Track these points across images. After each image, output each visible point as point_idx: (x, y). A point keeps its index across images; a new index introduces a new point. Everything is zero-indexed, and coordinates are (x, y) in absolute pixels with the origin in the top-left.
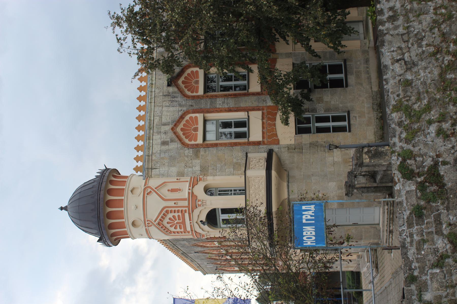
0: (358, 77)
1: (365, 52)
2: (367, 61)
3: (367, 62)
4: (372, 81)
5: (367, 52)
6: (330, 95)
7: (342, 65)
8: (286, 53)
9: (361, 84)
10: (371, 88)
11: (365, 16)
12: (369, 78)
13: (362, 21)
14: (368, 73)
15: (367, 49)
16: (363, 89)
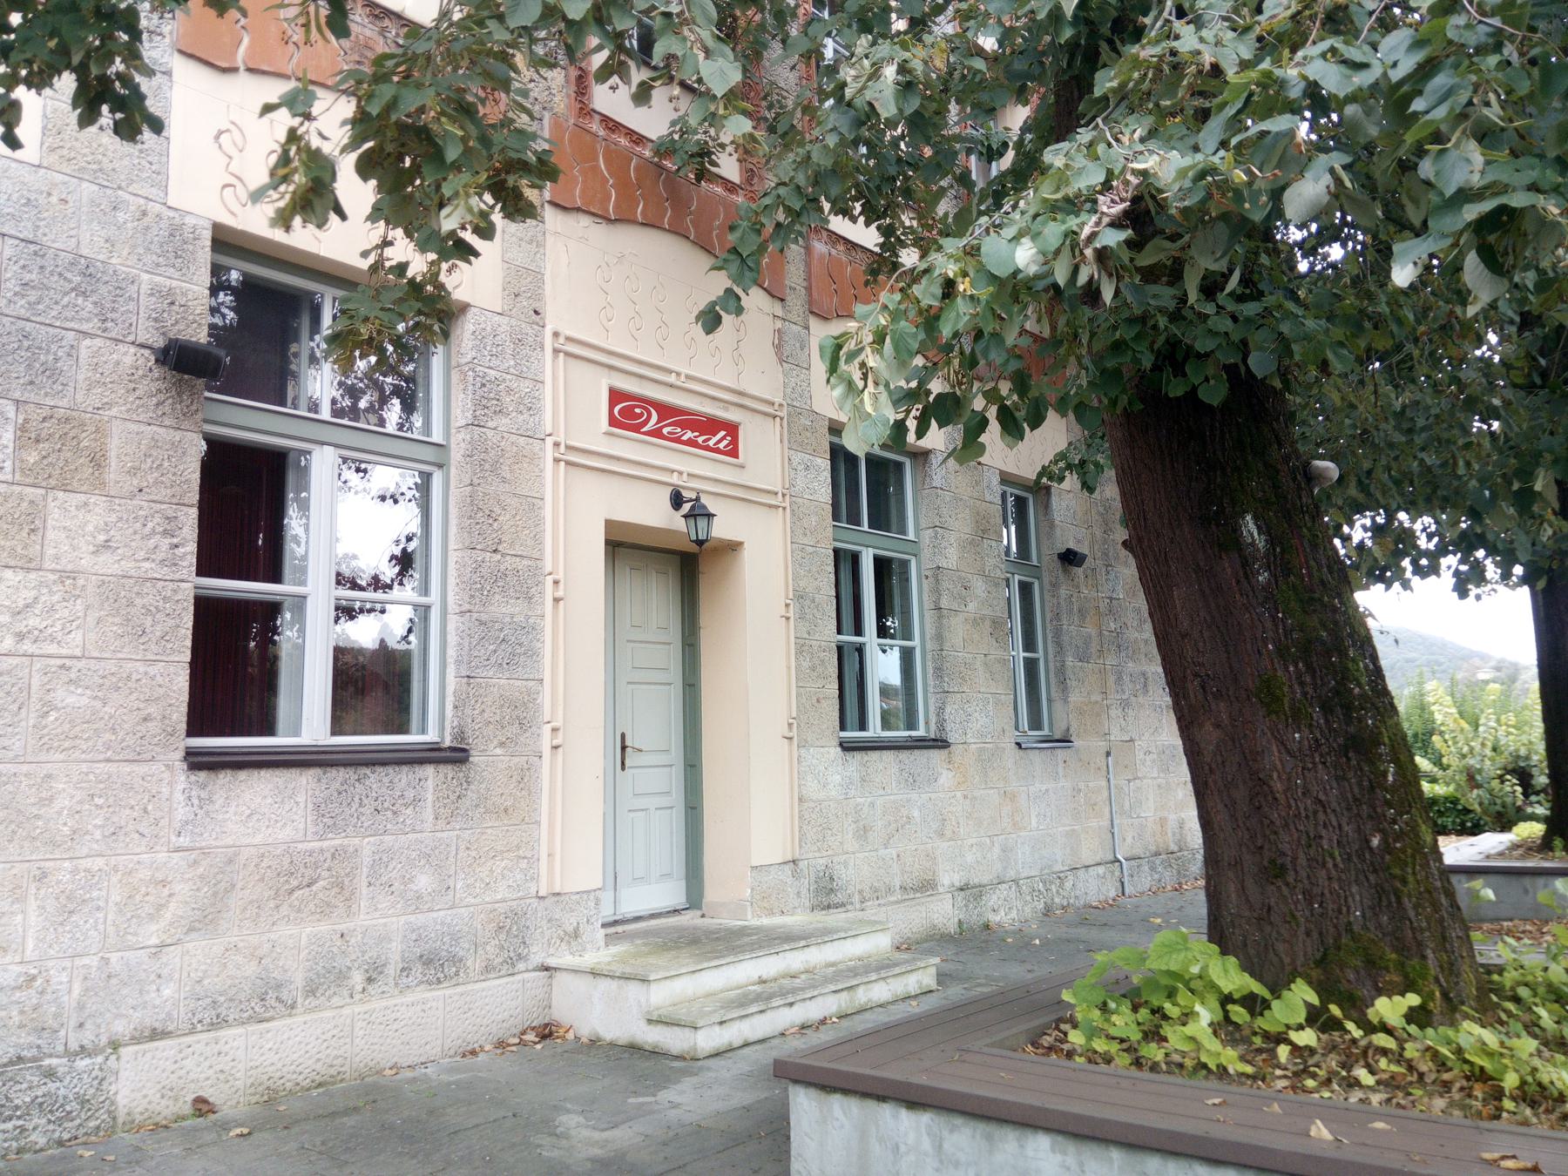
0: (300, 880)
1: (510, 939)
2: (435, 964)
3: (427, 961)
4: (233, 1037)
5: (512, 962)
6: (108, 564)
7: (403, 729)
8: (538, 276)
9: (204, 921)
10: (156, 1035)
11: (753, 920)
12: (267, 1001)
13: (695, 898)
14: (325, 981)
15: (538, 956)
16: (152, 934)
